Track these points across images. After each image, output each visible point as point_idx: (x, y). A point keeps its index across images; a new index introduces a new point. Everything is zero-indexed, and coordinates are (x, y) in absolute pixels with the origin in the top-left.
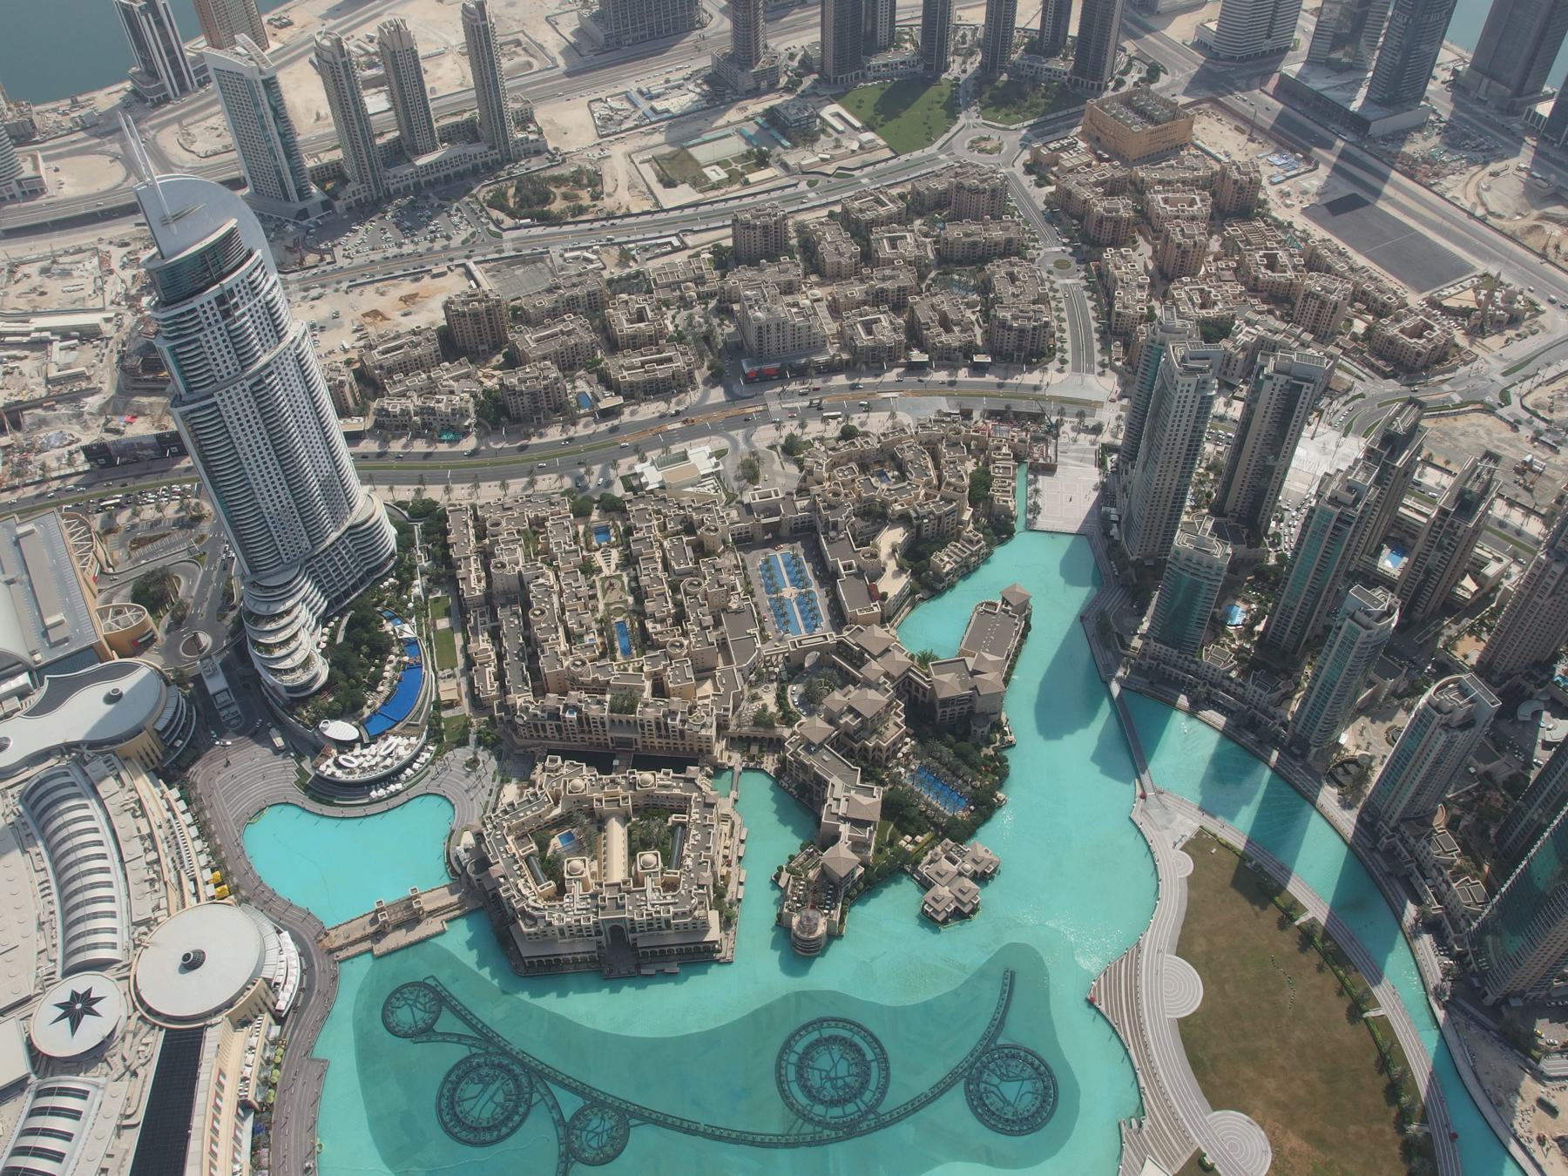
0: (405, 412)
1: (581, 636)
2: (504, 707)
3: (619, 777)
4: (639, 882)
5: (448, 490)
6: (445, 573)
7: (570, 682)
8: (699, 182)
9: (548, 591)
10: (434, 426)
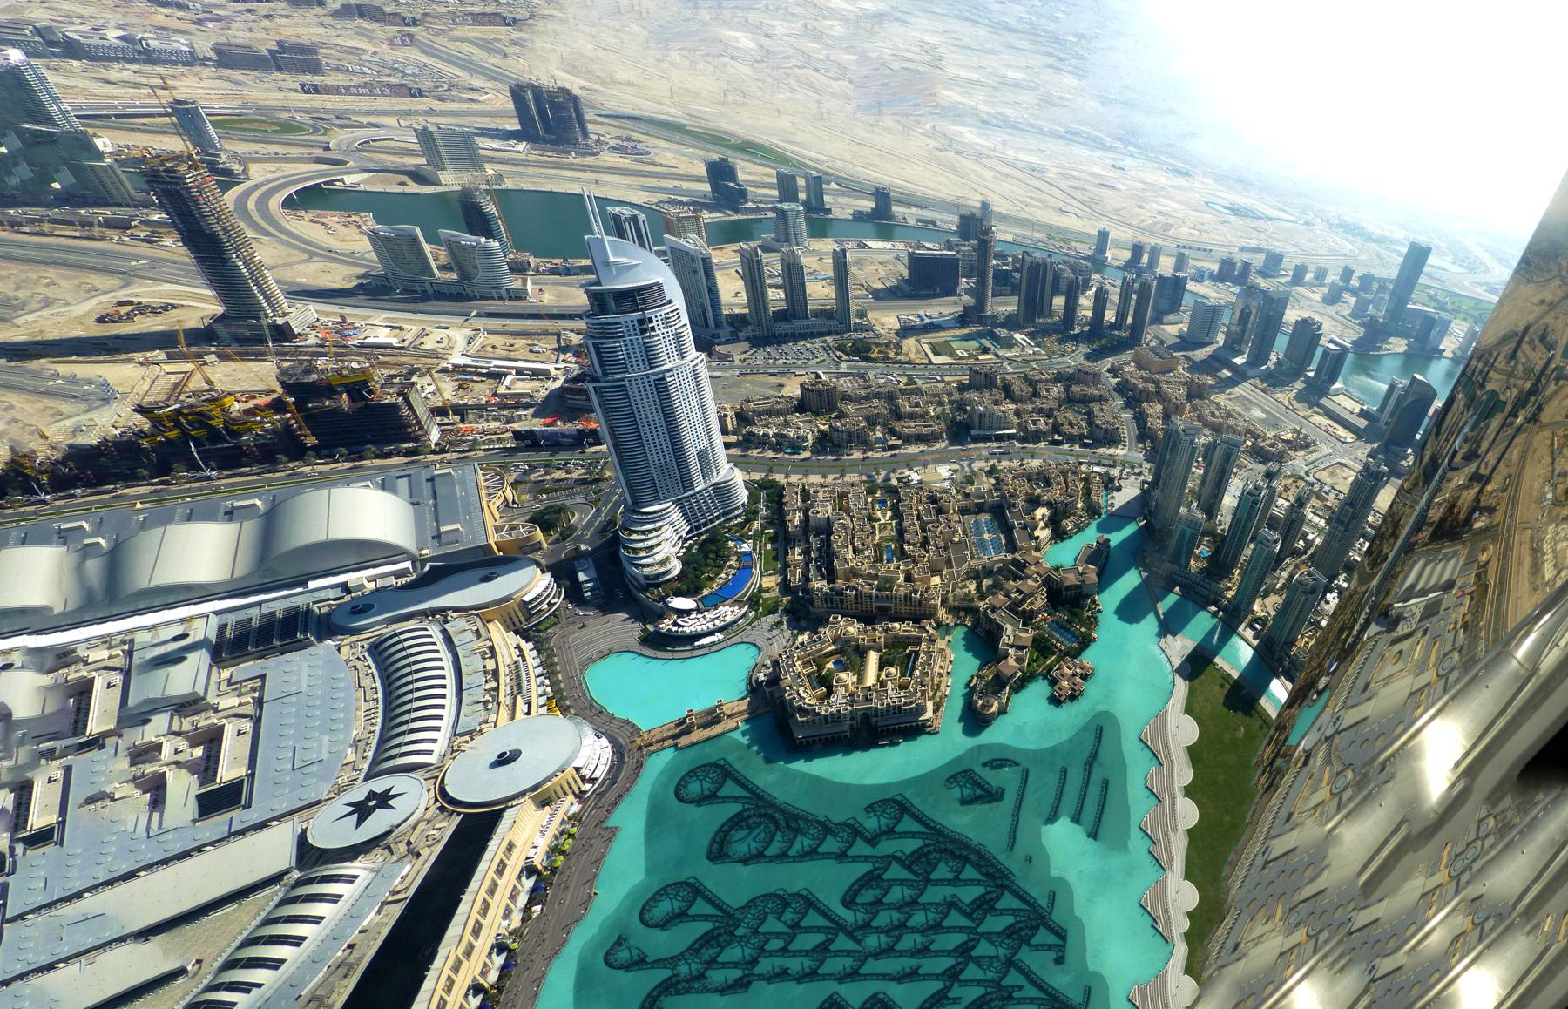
0: (766, 435)
1: (862, 551)
2: (807, 591)
3: (877, 626)
4: (883, 684)
5: (787, 476)
6: (778, 516)
7: (854, 573)
8: (952, 354)
9: (844, 527)
10: (780, 443)
